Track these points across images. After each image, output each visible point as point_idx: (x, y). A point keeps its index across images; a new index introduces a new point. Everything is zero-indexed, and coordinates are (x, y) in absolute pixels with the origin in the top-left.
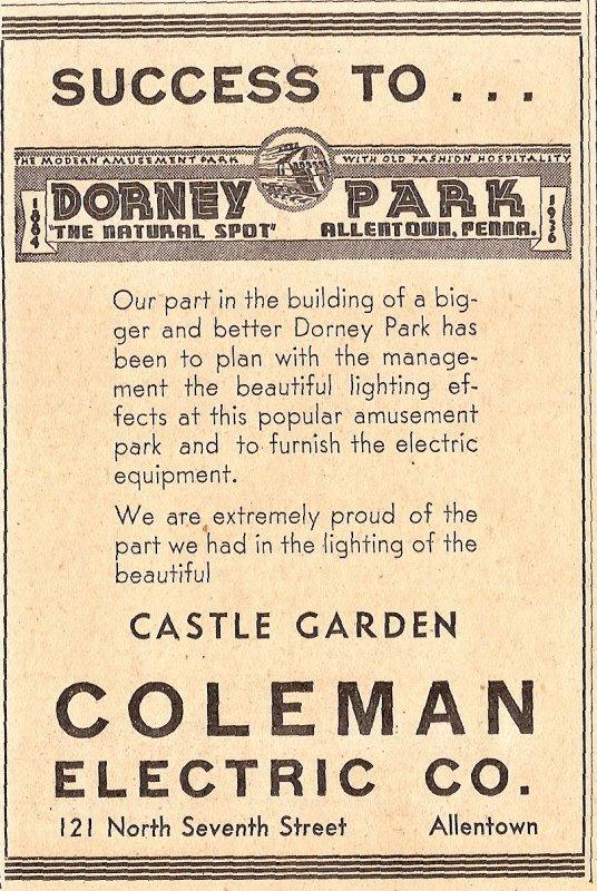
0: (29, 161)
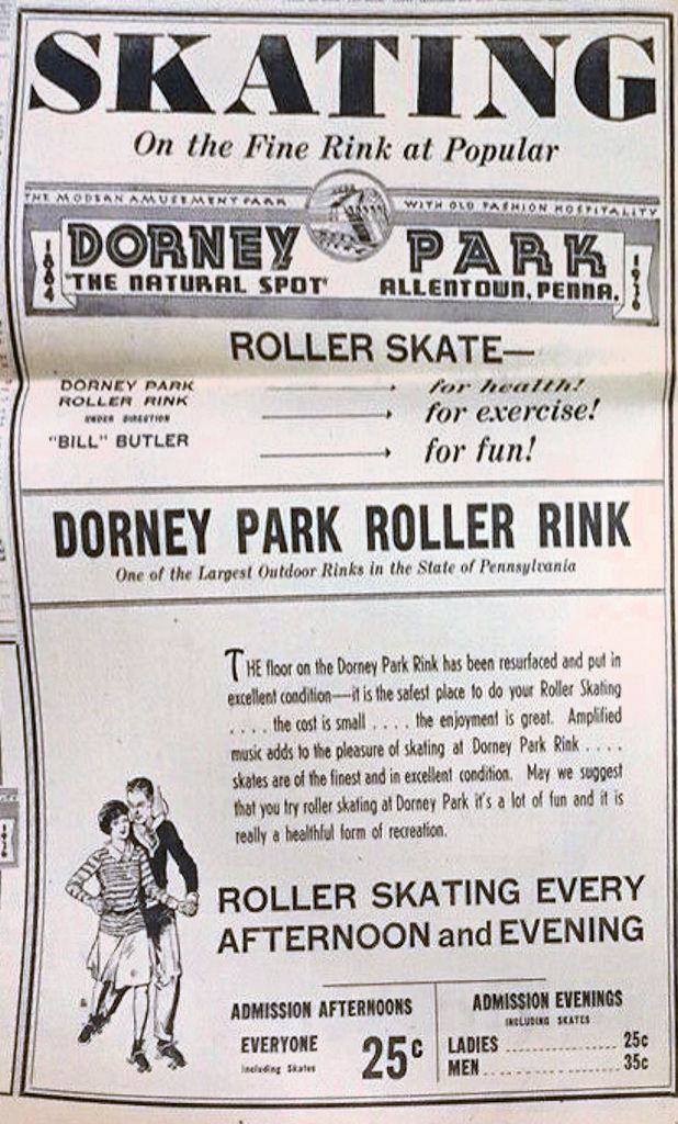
0: (42, 197)
